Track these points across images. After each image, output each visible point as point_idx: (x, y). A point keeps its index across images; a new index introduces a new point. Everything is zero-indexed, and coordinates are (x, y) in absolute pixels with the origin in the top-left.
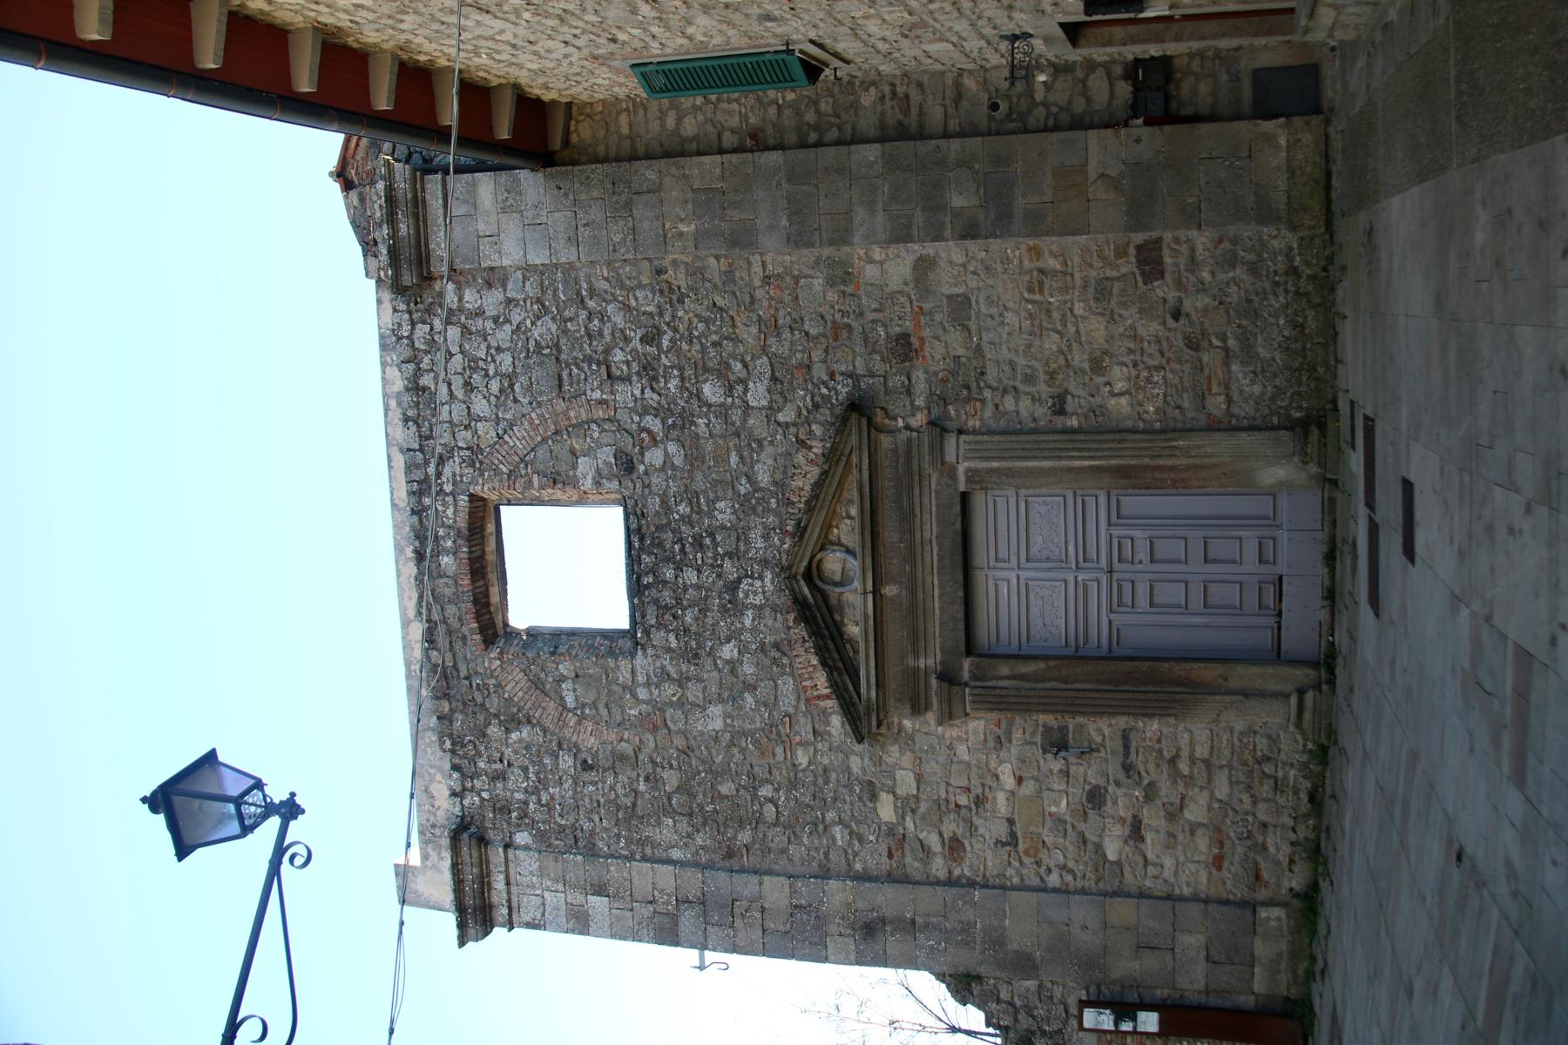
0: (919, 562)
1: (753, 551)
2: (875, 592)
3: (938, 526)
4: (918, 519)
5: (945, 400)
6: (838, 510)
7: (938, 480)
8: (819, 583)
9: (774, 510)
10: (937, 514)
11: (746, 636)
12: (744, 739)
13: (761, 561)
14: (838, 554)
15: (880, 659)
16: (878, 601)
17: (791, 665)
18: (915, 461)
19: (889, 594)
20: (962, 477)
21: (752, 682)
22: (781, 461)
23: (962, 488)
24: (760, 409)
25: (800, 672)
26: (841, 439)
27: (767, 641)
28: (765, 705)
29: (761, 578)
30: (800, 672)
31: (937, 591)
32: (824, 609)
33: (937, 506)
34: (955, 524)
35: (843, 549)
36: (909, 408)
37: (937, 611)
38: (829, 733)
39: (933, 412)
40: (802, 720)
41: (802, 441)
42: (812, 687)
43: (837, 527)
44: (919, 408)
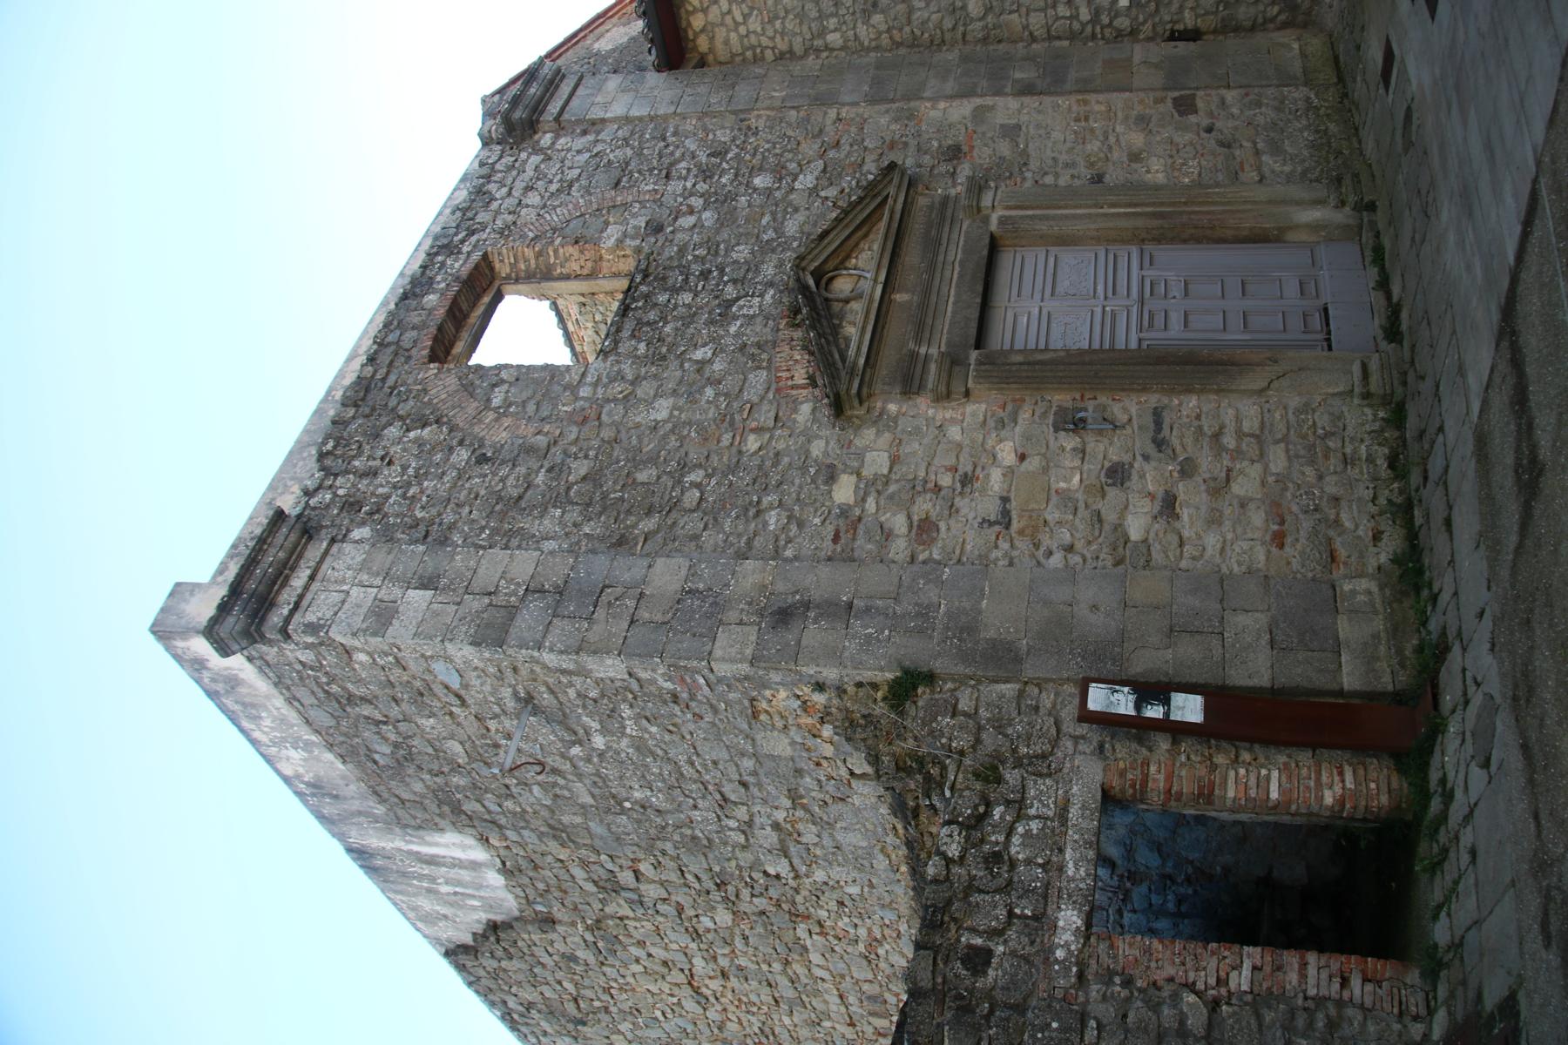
0: (938, 275)
31: (951, 299)
43: (856, 258)
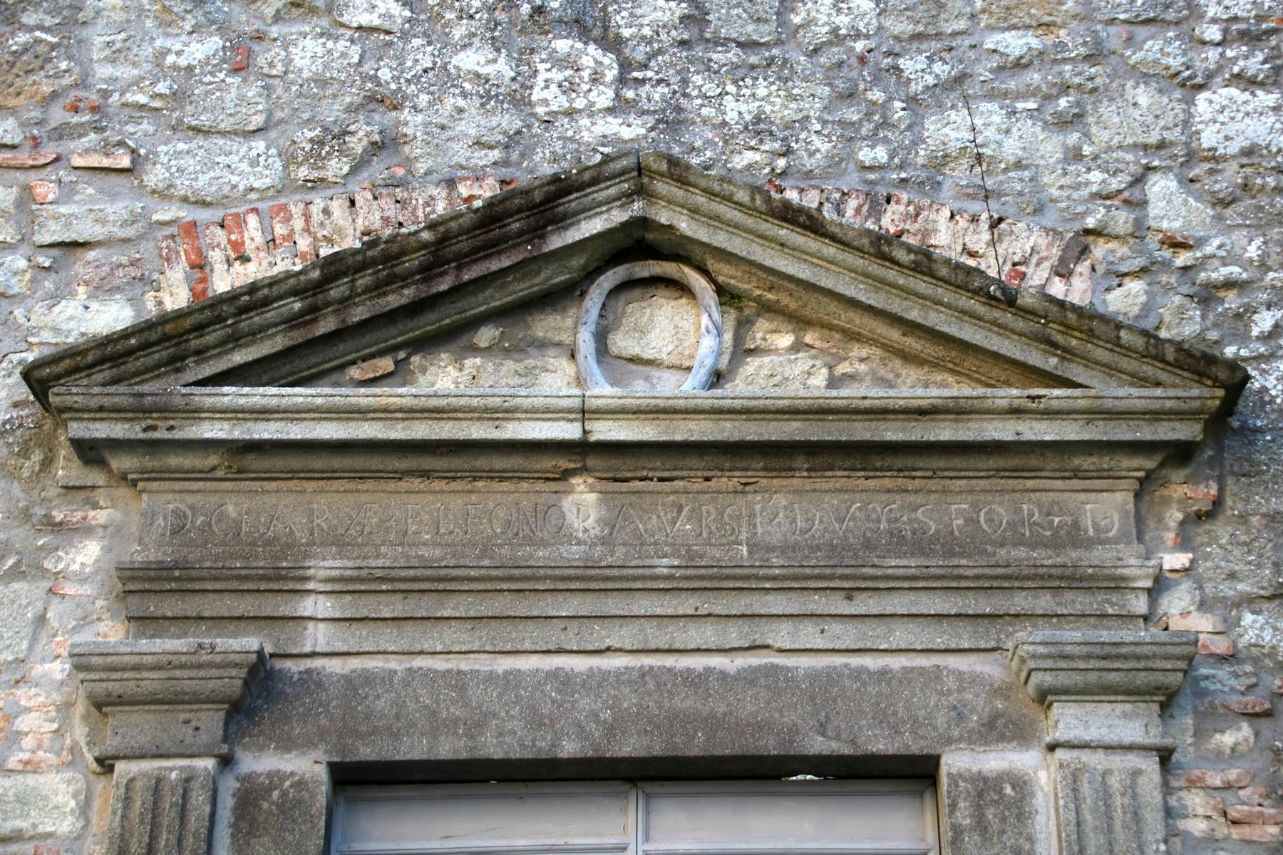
0: (687, 605)
1: (711, 89)
2: (582, 449)
3: (813, 675)
4: (839, 605)
5: (1268, 714)
6: (858, 351)
7: (975, 679)
8: (608, 280)
9: (851, 155)
10: (858, 674)
11: (421, 55)
12: (49, 21)
13: (679, 109)
14: (708, 343)
15: (337, 462)
16: (547, 463)
17: (317, 184)
18: (1044, 602)
19: (567, 503)
20: (995, 760)
21: (261, 61)
22: (1015, 182)
23: (954, 762)
24: (1186, 123)
25: (297, 210)
26: (1128, 350)
27: (405, 114)
28: (178, 97)
29: (620, 107)
30: (297, 210)
31: (579, 664)
32: (520, 289)
33: (884, 673)
34: (822, 729)
35: (724, 363)
36: (1227, 590)
37: (504, 664)
38: (55, 298)
39: (1223, 672)
40: (117, 209)
41: (1085, 250)
42: (237, 246)
43: (797, 347)
44: (1229, 626)
